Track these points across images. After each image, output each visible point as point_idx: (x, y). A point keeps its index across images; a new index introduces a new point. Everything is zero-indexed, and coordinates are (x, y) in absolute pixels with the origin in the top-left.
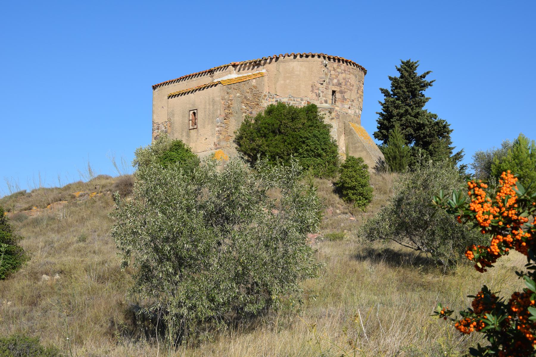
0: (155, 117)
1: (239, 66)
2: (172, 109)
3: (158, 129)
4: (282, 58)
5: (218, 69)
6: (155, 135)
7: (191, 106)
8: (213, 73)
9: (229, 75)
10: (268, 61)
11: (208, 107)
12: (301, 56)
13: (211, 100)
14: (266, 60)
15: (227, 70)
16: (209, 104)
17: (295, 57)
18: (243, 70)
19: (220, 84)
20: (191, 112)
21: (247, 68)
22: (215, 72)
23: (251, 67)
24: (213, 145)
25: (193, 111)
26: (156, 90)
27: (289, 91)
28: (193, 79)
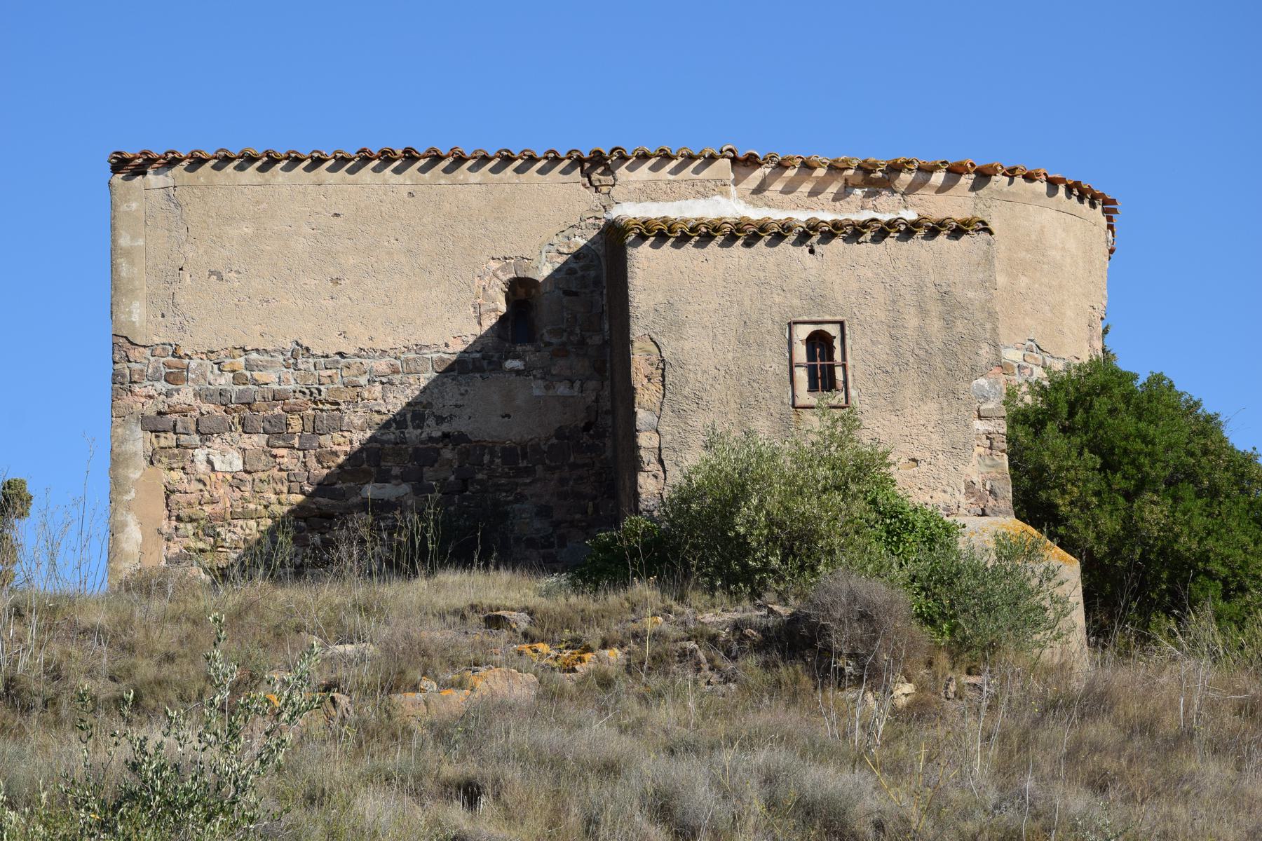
0: (137, 315)
1: (758, 174)
2: (660, 297)
3: (174, 377)
4: (1000, 180)
5: (645, 157)
6: (150, 409)
7: (796, 302)
8: (609, 171)
9: (718, 197)
10: (938, 178)
11: (912, 322)
12: (1069, 190)
13: (931, 291)
14: (928, 170)
15: (705, 174)
16: (923, 312)
17: (1053, 184)
18: (787, 191)
19: (985, 235)
20: (803, 332)
21: (806, 188)
22: (622, 172)
23: (834, 188)
24: (961, 498)
25: (811, 328)
26: (152, 178)
27: (1028, 320)
28: (463, 172)
